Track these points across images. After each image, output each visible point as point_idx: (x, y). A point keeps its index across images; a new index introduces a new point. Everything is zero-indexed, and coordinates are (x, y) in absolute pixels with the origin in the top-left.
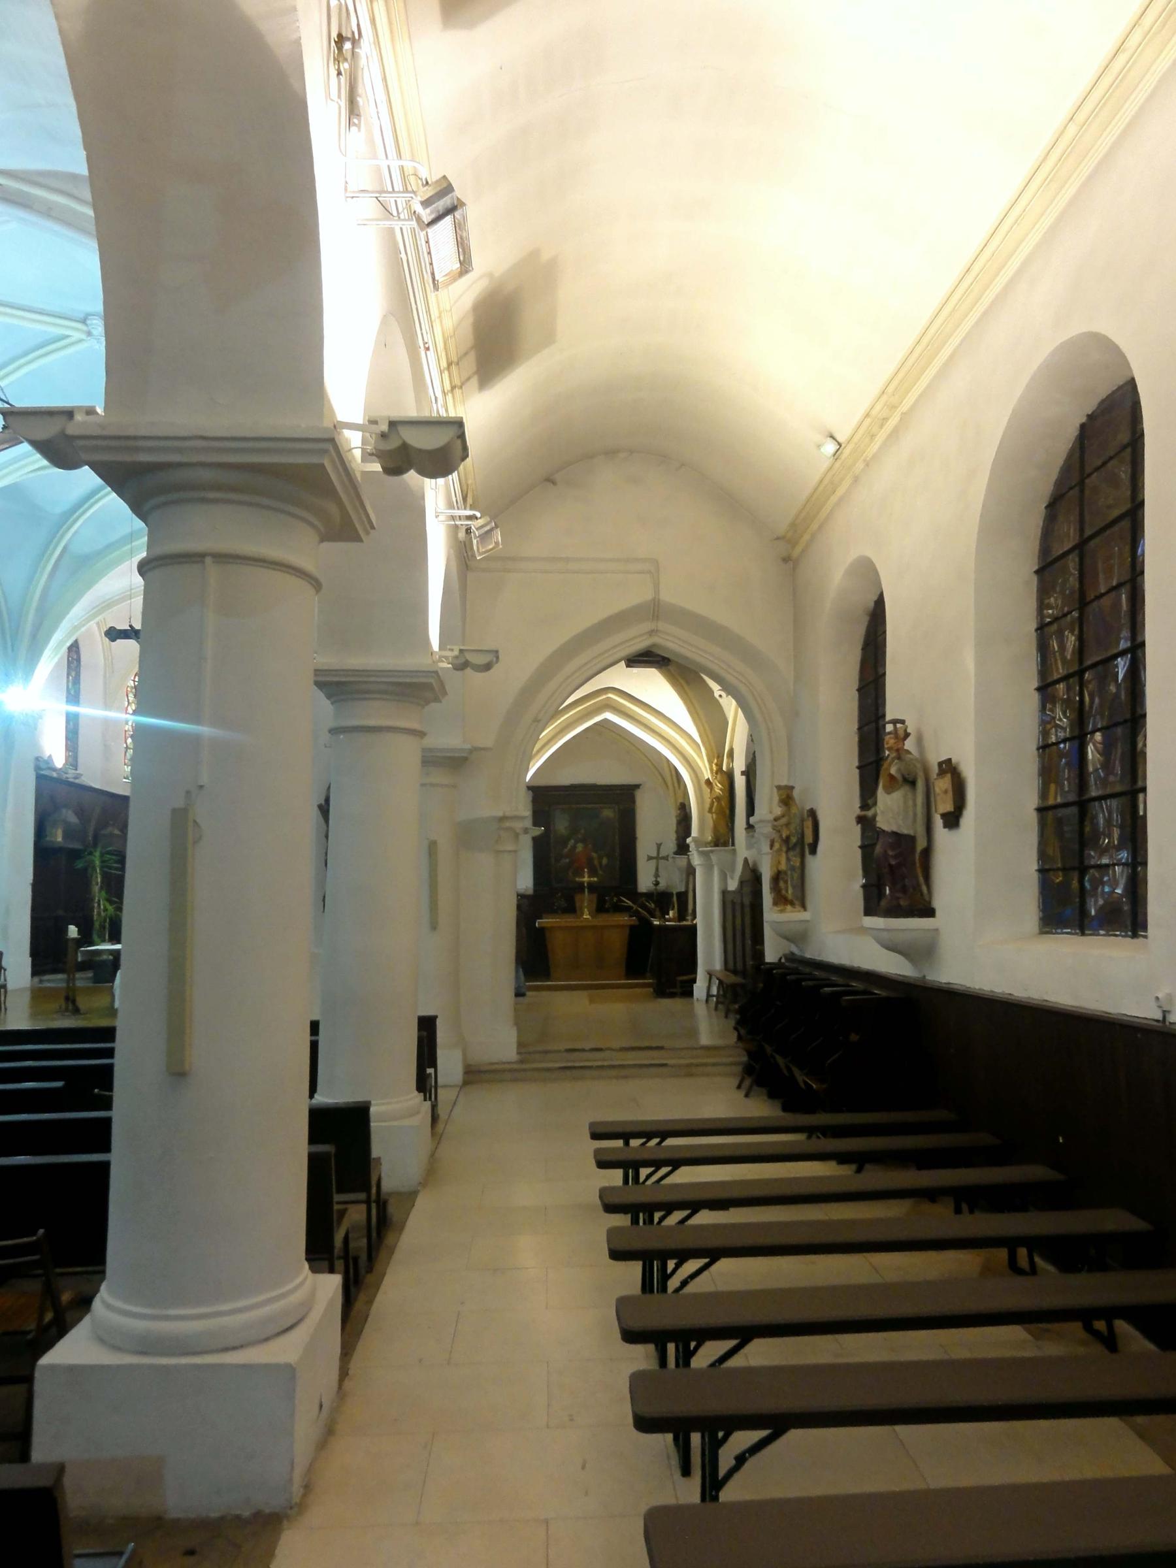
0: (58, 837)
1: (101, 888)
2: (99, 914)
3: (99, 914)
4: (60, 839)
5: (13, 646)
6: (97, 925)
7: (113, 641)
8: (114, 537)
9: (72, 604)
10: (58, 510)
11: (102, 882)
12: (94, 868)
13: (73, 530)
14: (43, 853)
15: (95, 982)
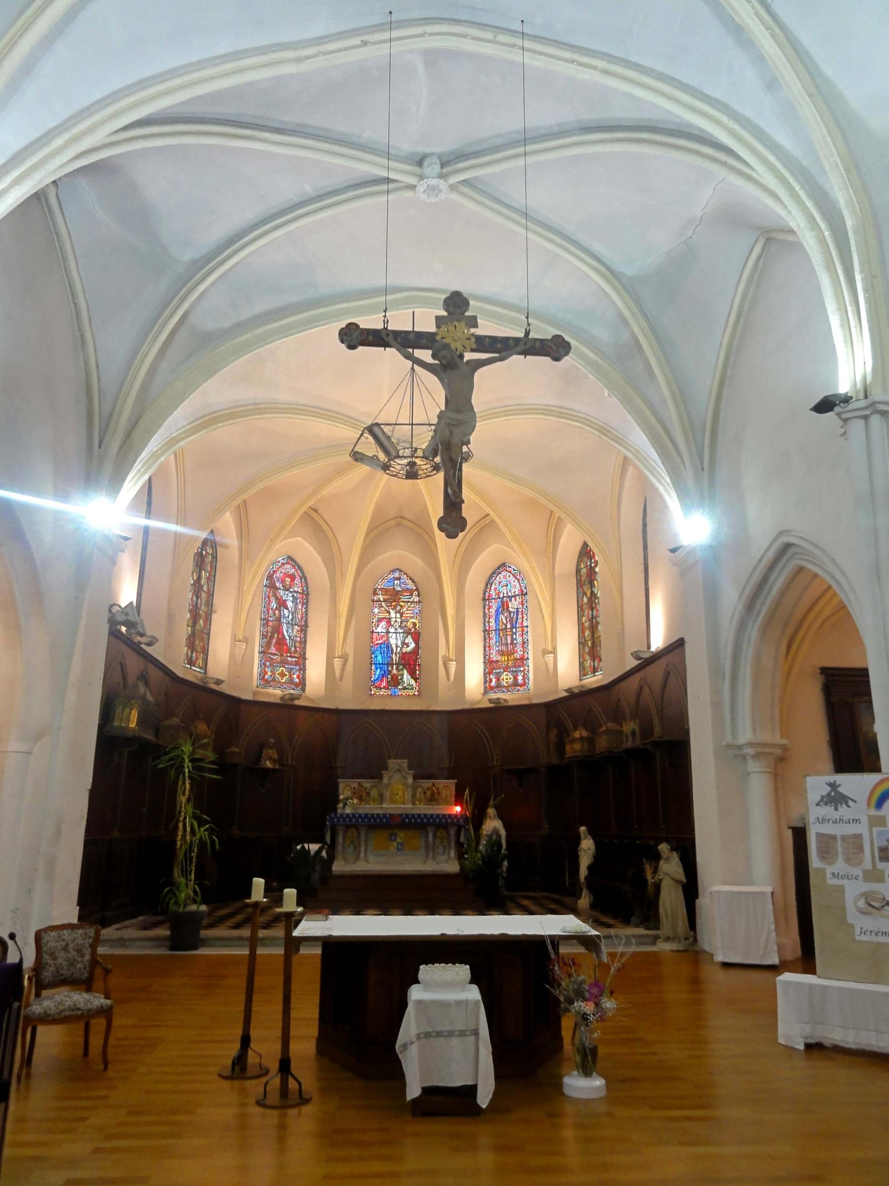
0: (131, 720)
1: (188, 800)
2: (184, 836)
3: (184, 836)
4: (133, 725)
5: (101, 441)
6: (181, 855)
7: (352, 347)
8: (246, 314)
9: (174, 406)
10: (188, 256)
11: (191, 790)
12: (180, 769)
13: (202, 288)
14: (109, 743)
15: (173, 948)
